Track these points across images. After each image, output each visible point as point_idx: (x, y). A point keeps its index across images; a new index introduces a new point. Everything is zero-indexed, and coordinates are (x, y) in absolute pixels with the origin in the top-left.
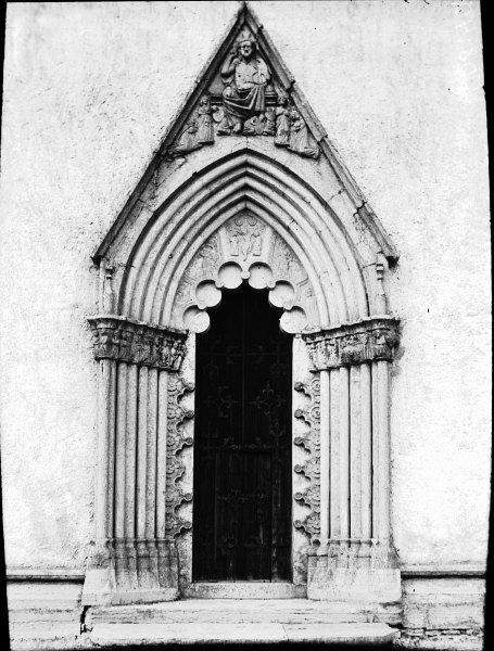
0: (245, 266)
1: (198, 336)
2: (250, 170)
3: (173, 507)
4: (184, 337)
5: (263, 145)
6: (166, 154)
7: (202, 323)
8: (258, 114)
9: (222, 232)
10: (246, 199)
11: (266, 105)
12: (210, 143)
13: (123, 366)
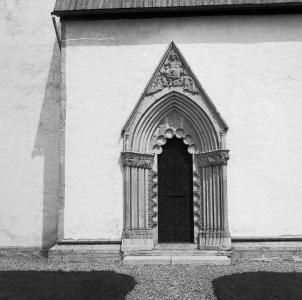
0: (174, 130)
1: (159, 156)
2: (175, 98)
3: (150, 209)
5: (180, 90)
6: (146, 94)
7: (160, 151)
8: (178, 79)
9: (166, 119)
10: (174, 107)
11: (181, 75)
13: (133, 168)
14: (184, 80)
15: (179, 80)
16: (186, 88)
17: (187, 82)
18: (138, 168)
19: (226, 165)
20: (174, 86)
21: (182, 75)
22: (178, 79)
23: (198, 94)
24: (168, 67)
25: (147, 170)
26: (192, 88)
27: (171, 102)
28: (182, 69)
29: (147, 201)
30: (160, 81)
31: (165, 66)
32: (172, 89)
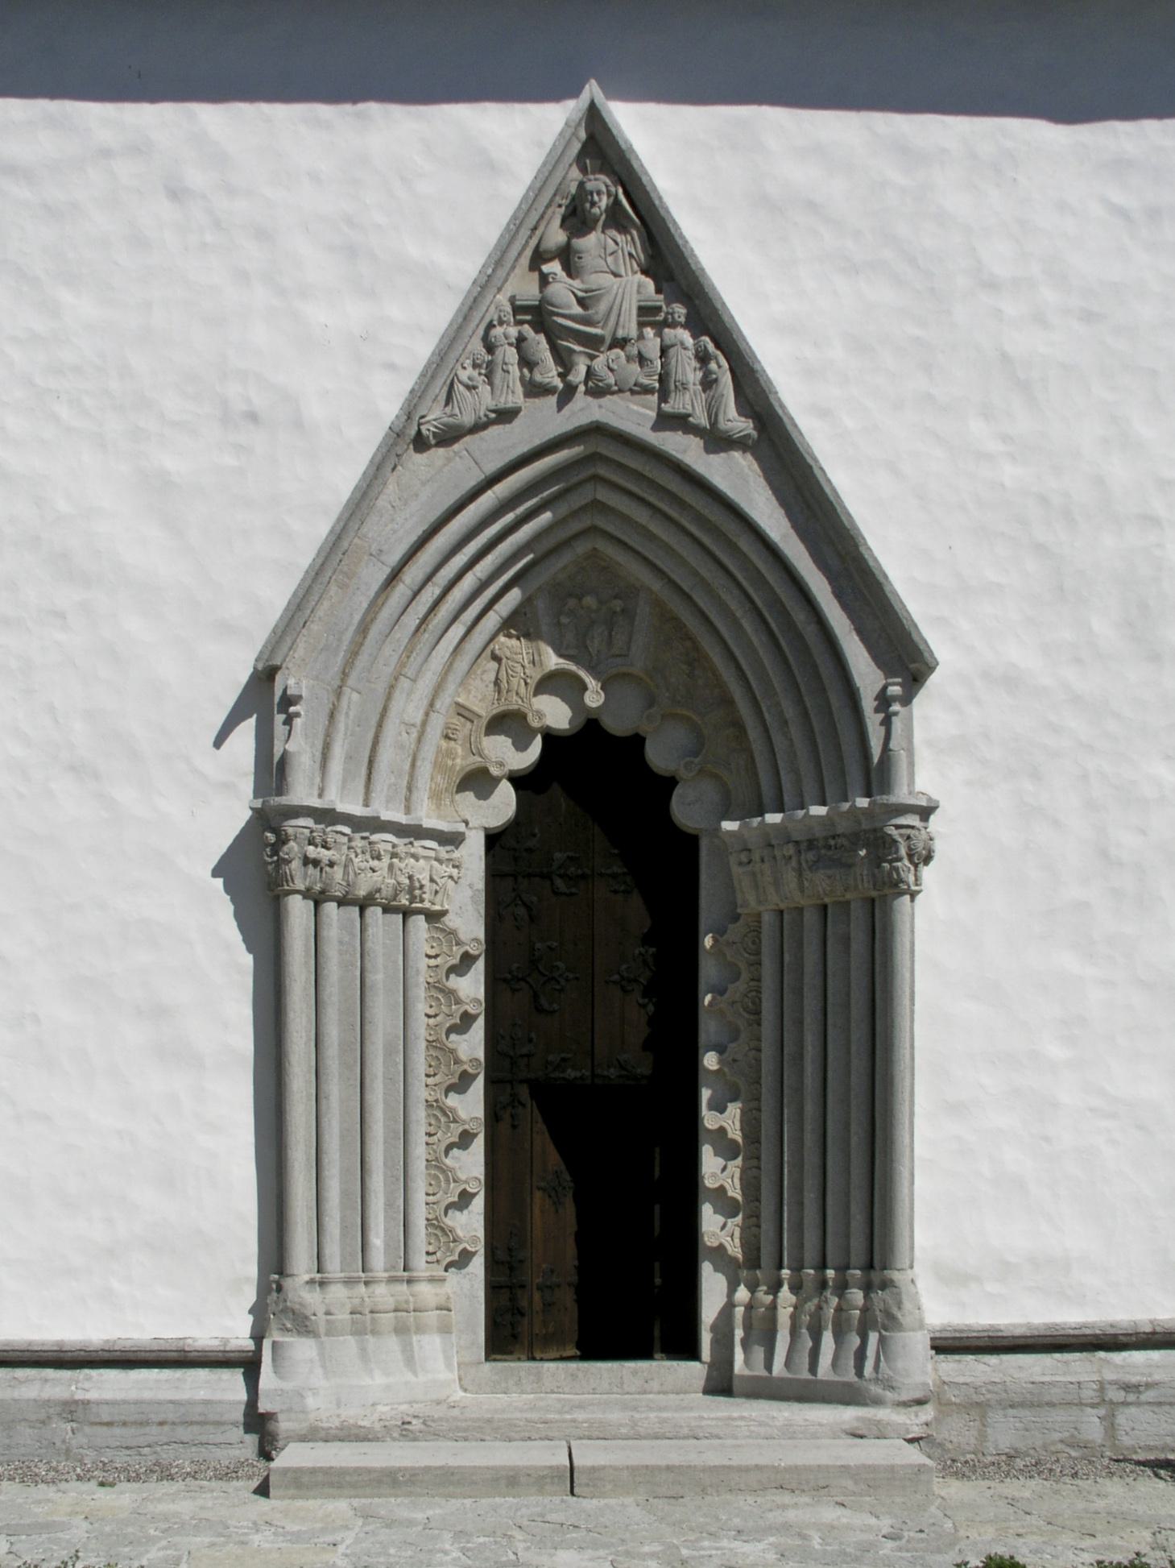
1: (493, 840)
2: (602, 471)
7: (503, 805)
8: (620, 343)
11: (641, 325)
12: (505, 416)
13: (330, 908)
14: (664, 351)
16: (677, 404)
17: (688, 371)
18: (363, 905)
19: (913, 895)
20: (598, 391)
22: (620, 343)
25: (419, 922)
26: (713, 412)
27: (577, 500)
29: (420, 1114)
30: (512, 355)
32: (584, 410)
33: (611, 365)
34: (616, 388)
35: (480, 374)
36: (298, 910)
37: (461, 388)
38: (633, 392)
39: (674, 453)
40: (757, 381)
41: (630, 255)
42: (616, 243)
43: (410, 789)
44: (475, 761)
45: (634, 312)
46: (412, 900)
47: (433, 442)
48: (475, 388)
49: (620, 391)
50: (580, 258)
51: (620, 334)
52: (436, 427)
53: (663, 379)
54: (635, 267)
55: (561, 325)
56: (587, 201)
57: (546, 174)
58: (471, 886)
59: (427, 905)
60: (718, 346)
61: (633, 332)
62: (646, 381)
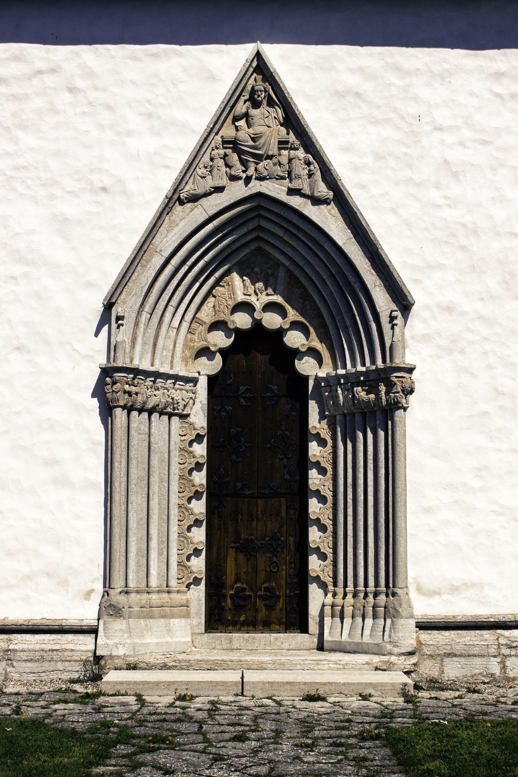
1: (212, 380)
2: (263, 213)
4: (194, 381)
8: (270, 157)
11: (280, 149)
12: (220, 189)
13: (135, 413)
14: (290, 160)
15: (275, 160)
16: (296, 184)
17: (301, 170)
18: (150, 412)
19: (405, 409)
21: (285, 149)
22: (270, 157)
23: (328, 204)
24: (242, 123)
26: (312, 186)
27: (251, 226)
28: (283, 130)
29: (174, 512)
30: (221, 162)
31: (236, 119)
32: (256, 187)
33: (266, 167)
34: (268, 177)
35: (207, 171)
36: (120, 414)
37: (199, 178)
38: (277, 179)
39: (294, 206)
40: (332, 174)
41: (275, 118)
42: (269, 113)
43: (172, 357)
44: (203, 344)
45: (276, 143)
46: (174, 409)
47: (186, 201)
48: (204, 177)
49: (270, 178)
50: (252, 119)
51: (270, 153)
52: (187, 195)
53: (290, 173)
54: (278, 123)
55: (243, 150)
56: (256, 94)
57: (237, 83)
58: (201, 402)
59: (180, 411)
60: (314, 158)
61: (276, 152)
62: (282, 174)
